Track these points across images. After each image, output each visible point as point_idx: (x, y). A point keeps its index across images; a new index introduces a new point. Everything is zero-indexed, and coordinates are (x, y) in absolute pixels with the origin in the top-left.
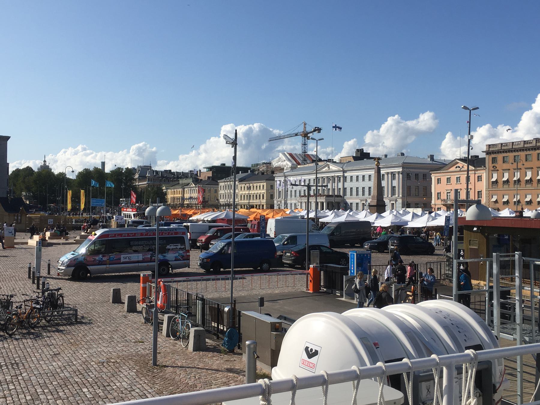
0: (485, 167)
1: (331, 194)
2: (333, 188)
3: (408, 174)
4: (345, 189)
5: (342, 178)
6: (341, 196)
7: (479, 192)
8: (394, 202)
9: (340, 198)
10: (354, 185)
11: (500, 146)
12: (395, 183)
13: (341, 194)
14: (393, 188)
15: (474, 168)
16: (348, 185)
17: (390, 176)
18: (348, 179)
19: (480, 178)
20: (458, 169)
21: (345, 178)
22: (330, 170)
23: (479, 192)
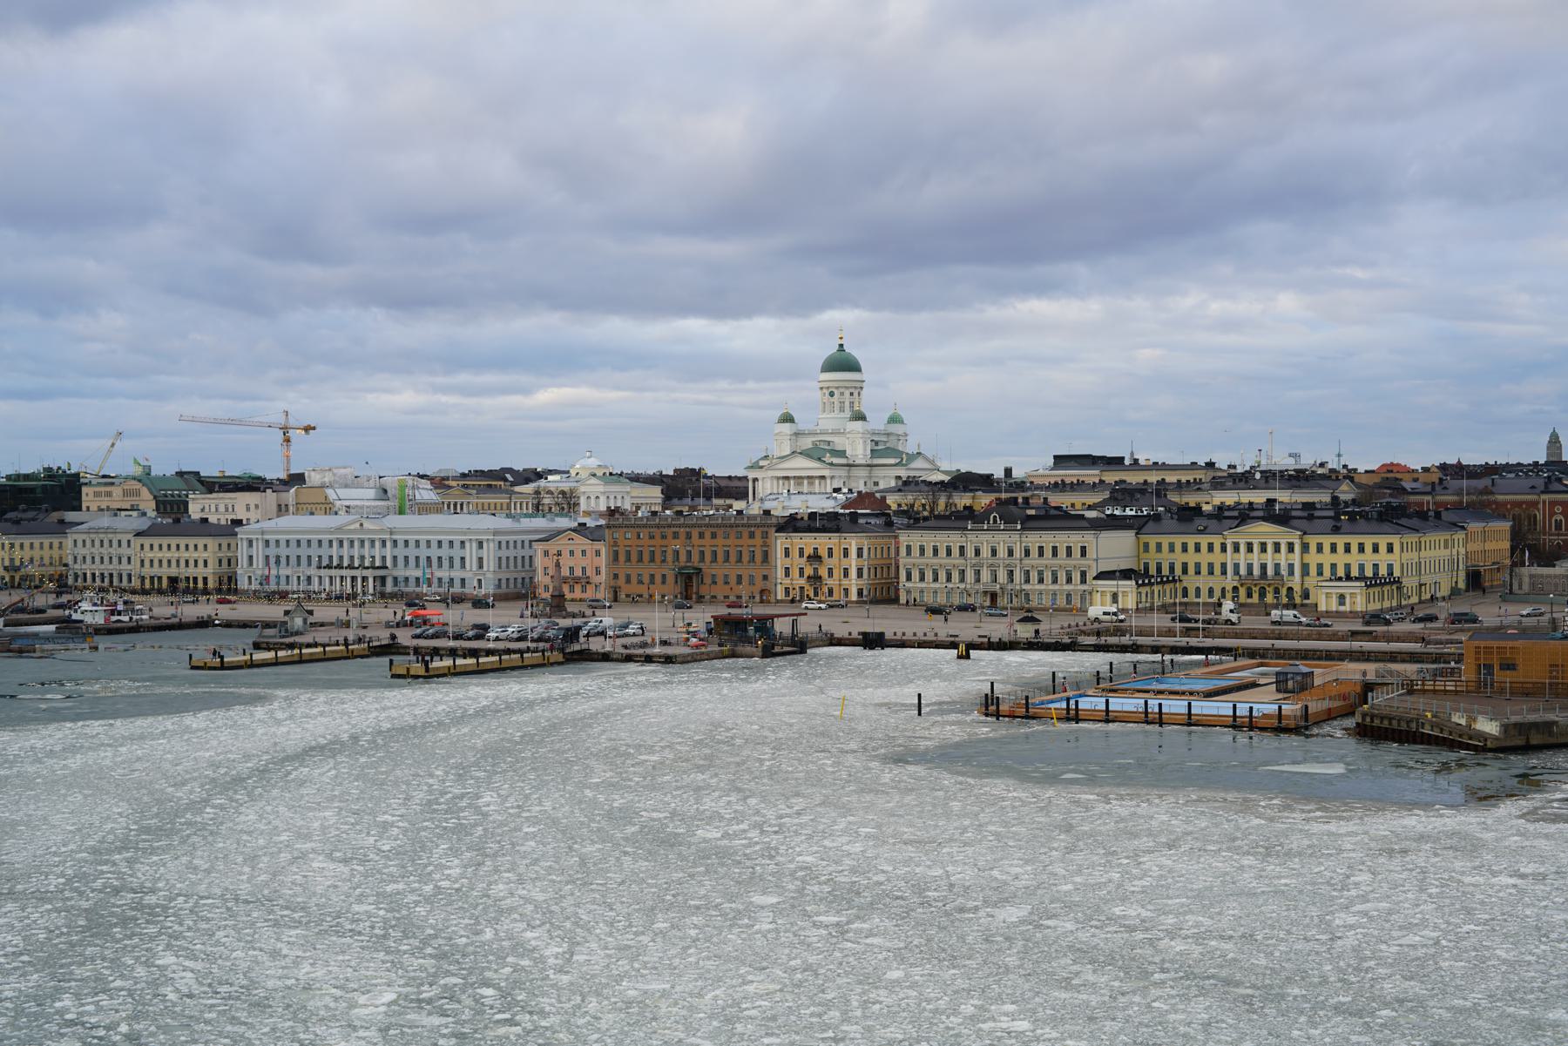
17: (475, 545)
19: (598, 553)
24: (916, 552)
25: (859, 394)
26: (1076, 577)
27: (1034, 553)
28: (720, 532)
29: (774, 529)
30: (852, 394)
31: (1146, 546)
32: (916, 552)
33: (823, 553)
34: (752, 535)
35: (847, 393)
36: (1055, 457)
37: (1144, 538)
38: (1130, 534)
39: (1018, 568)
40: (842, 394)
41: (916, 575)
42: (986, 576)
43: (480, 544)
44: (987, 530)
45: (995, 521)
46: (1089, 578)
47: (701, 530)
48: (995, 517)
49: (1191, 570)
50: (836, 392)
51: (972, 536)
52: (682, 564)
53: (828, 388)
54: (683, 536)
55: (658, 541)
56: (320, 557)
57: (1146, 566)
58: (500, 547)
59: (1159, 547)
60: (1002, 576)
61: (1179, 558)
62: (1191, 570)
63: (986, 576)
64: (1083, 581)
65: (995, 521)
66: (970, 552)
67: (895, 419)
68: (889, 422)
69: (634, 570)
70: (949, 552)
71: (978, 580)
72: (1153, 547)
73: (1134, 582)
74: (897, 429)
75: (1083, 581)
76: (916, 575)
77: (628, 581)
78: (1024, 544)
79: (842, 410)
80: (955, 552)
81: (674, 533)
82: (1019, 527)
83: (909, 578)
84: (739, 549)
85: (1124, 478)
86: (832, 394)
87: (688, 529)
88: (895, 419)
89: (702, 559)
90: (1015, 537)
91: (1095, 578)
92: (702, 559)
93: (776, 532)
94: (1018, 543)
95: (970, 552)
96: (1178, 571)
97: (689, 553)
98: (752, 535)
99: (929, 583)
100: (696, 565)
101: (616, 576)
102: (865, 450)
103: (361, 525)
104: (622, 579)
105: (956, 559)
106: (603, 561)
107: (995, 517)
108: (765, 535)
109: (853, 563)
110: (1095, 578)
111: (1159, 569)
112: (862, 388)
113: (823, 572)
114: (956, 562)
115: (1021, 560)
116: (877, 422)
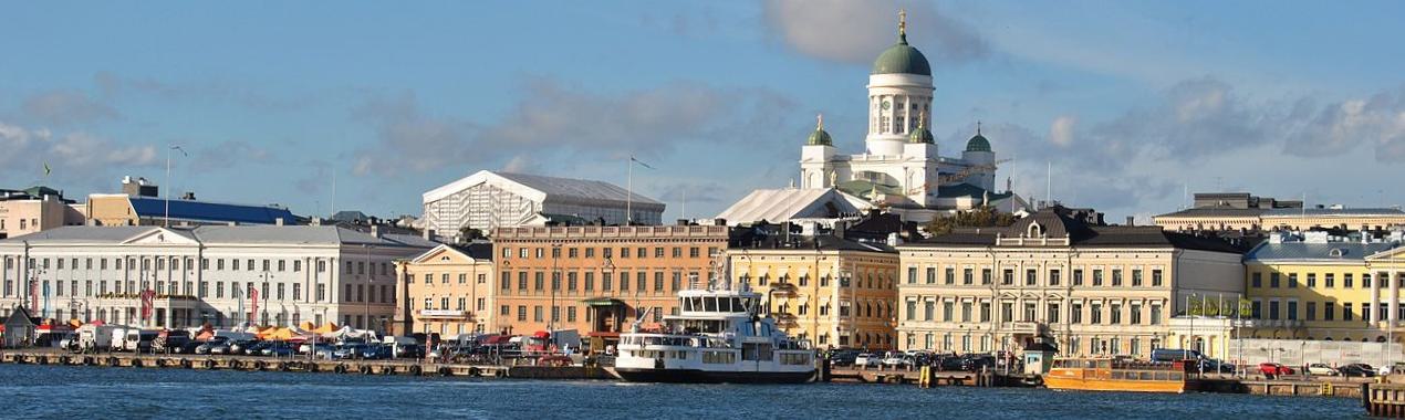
0: (491, 260)
1: (180, 293)
2: (144, 279)
3: (349, 263)
4: (203, 286)
5: (196, 263)
6: (193, 298)
7: (480, 299)
8: (322, 313)
9: (192, 302)
10: (228, 276)
11: (515, 231)
12: (324, 278)
13: (195, 293)
14: (320, 288)
15: (472, 260)
16: (211, 276)
17: (312, 264)
18: (213, 264)
19: (482, 278)
20: (446, 261)
21: (204, 263)
22: (165, 243)
23: (480, 299)
24: (922, 276)
25: (926, 107)
27: (1088, 278)
29: (725, 245)
32: (922, 276)
34: (694, 252)
36: (1198, 197)
38: (1237, 257)
39: (1065, 302)
41: (920, 309)
43: (320, 265)
44: (1023, 246)
47: (624, 245)
52: (598, 294)
53: (882, 97)
54: (599, 253)
55: (565, 262)
56: (103, 282)
58: (350, 271)
67: (979, 143)
68: (969, 149)
69: (531, 299)
70: (968, 278)
74: (978, 157)
76: (920, 309)
77: (522, 317)
78: (1073, 268)
79: (898, 129)
80: (978, 277)
81: (588, 250)
82: (1067, 243)
83: (910, 316)
85: (1288, 224)
86: (883, 106)
87: (606, 245)
88: (979, 143)
89: (624, 286)
90: (1063, 257)
92: (624, 286)
94: (1066, 265)
97: (607, 278)
98: (694, 252)
99: (938, 324)
100: (617, 295)
101: (505, 310)
103: (162, 237)
104: (514, 312)
105: (979, 290)
106: (488, 290)
109: (832, 294)
112: (931, 99)
114: (979, 292)
115: (1071, 289)
116: (953, 147)
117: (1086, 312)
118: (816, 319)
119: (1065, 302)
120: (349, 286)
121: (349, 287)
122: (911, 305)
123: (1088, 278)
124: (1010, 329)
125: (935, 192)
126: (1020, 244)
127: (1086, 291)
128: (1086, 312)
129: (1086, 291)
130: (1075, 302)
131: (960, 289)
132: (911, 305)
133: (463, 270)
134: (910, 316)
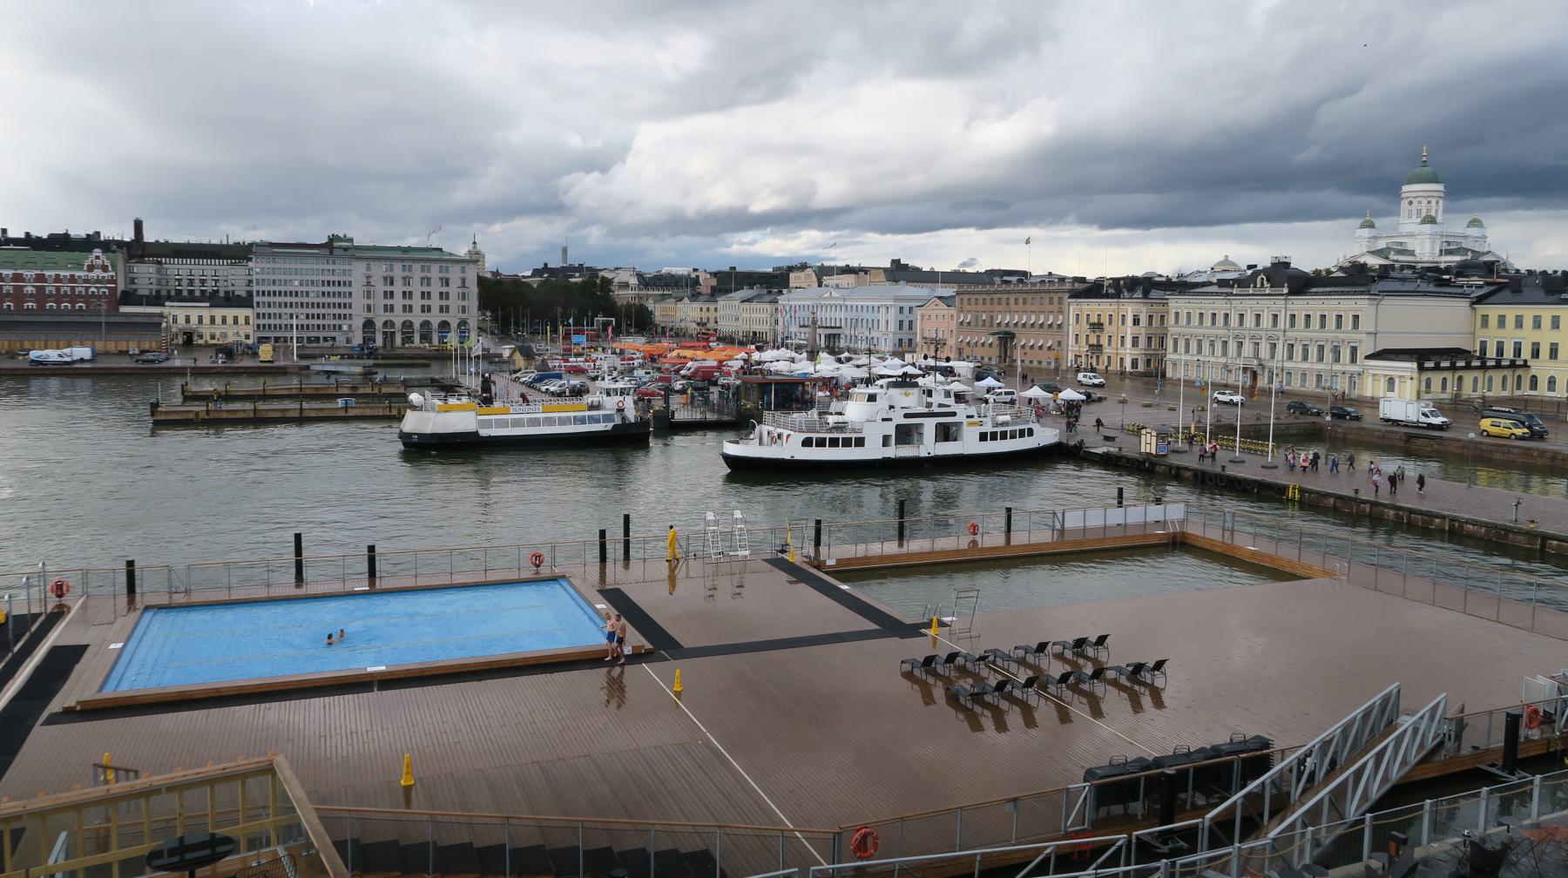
20: (937, 307)
26: (1346, 354)
27: (1301, 322)
28: (1029, 297)
29: (1067, 295)
30: (1429, 202)
31: (1485, 319)
33: (1105, 320)
35: (1424, 202)
37: (1483, 309)
39: (1281, 341)
40: (1420, 202)
41: (1181, 344)
42: (1248, 349)
45: (1262, 285)
46: (1360, 355)
48: (1263, 279)
49: (1545, 352)
50: (1413, 200)
51: (1236, 303)
57: (1483, 345)
59: (1502, 321)
60: (1264, 351)
61: (1527, 337)
62: (1545, 352)
63: (1248, 349)
64: (1353, 360)
65: (1262, 285)
66: (1234, 321)
71: (1239, 354)
72: (1493, 321)
73: (1415, 365)
75: (1353, 360)
76: (1181, 344)
78: (1289, 313)
82: (1286, 291)
83: (1175, 350)
84: (991, 314)
91: (1368, 357)
93: (1069, 298)
94: (1283, 312)
95: (1234, 321)
96: (1526, 354)
102: (1433, 249)
107: (1263, 279)
108: (1061, 300)
110: (1368, 357)
111: (1500, 351)
113: (1104, 341)
114: (1220, 332)
115: (1285, 331)
117: (1298, 350)
118: (1117, 349)
119: (1281, 341)
120: (901, 322)
121: (901, 322)
122: (1176, 342)
123: (1301, 322)
124: (1241, 362)
125: (1437, 251)
126: (1251, 292)
127: (1299, 333)
128: (1298, 350)
129: (1315, 332)
130: (1289, 342)
131: (1207, 330)
132: (1176, 342)
133: (944, 312)
134: (1175, 350)
